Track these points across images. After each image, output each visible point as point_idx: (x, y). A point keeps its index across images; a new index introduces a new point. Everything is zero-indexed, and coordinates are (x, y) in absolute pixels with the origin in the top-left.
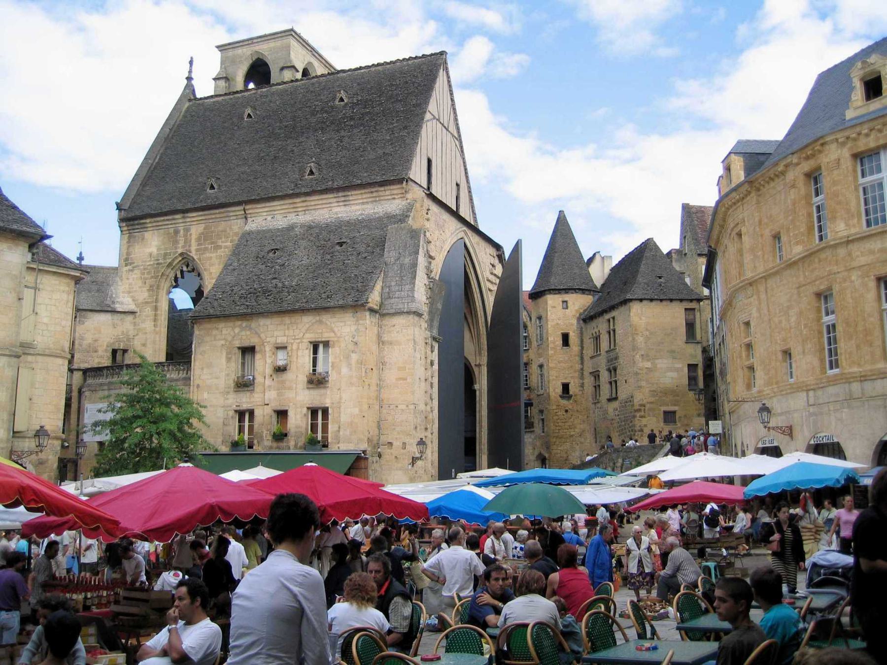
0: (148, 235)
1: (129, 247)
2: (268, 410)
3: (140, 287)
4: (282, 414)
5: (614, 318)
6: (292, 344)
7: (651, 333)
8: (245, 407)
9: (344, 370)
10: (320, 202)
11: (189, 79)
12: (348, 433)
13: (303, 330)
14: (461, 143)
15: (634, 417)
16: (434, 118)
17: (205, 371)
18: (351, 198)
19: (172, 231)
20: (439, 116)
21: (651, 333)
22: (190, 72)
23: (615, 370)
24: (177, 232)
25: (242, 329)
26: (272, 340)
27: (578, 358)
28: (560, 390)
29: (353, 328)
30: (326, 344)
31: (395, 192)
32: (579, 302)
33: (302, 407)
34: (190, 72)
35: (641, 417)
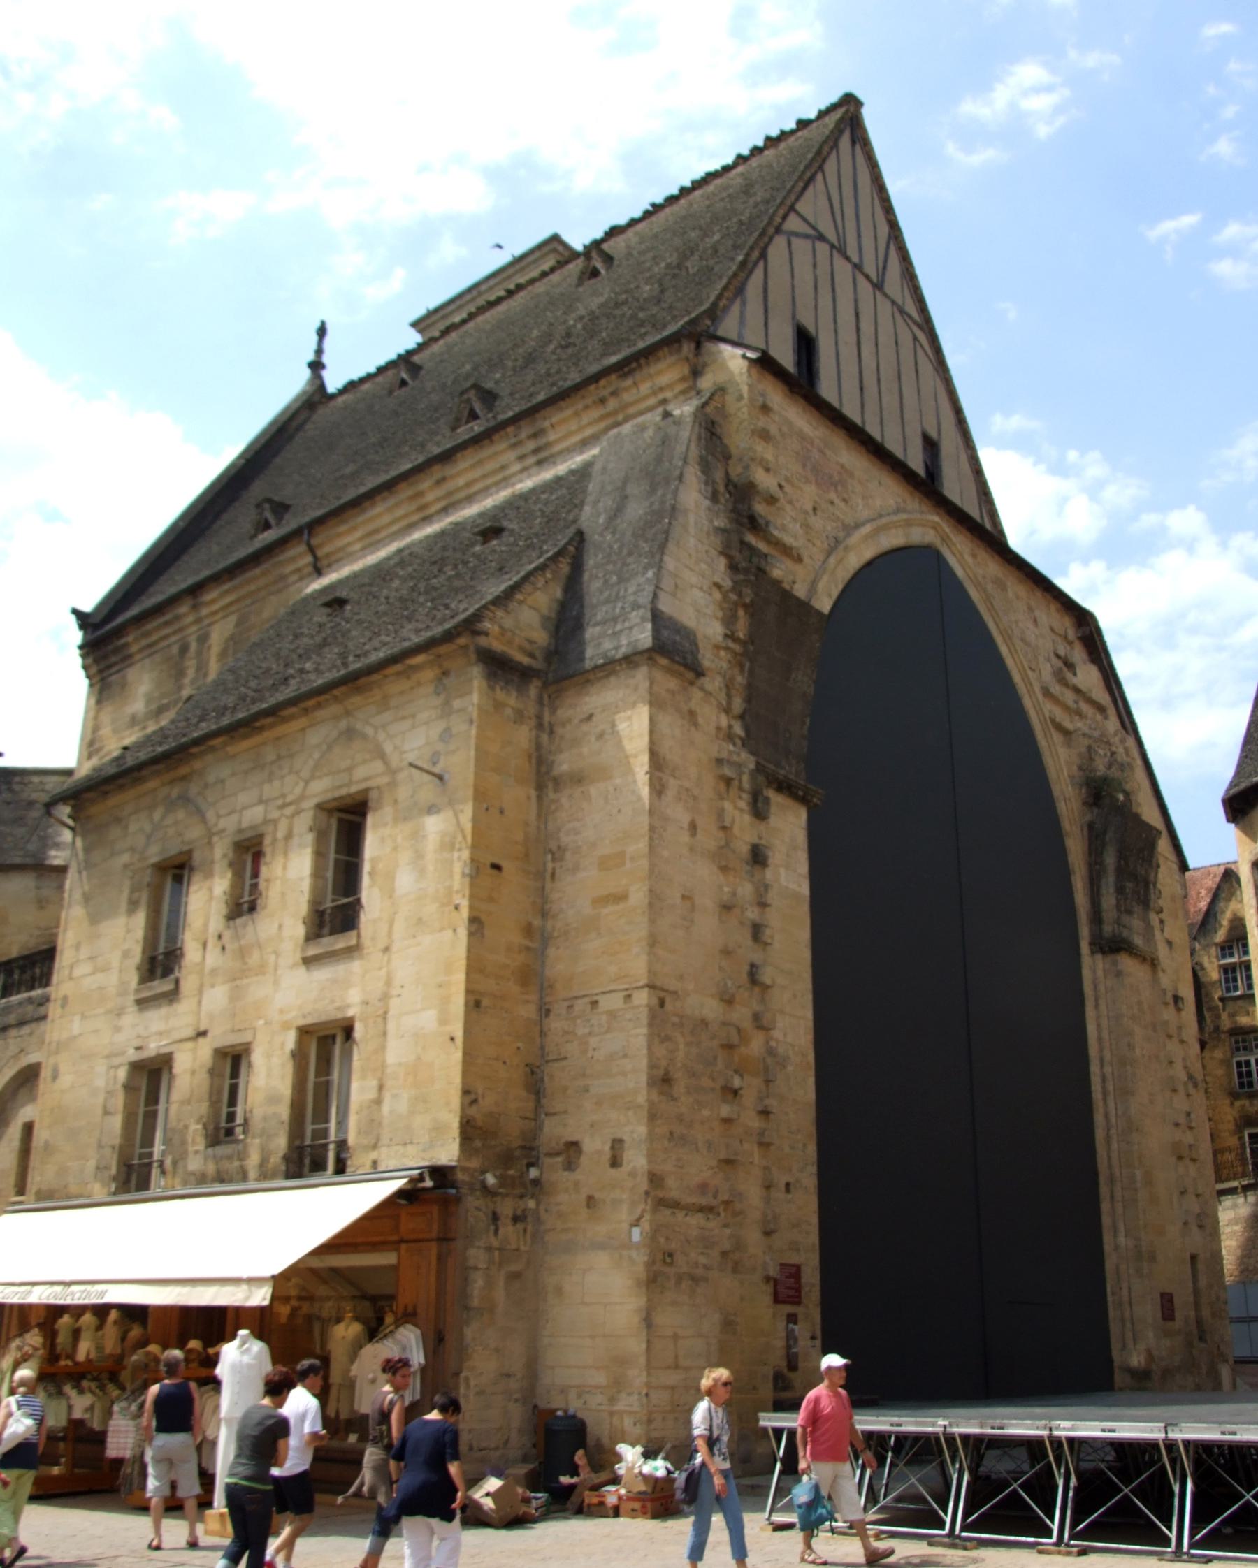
0: (132, 674)
2: (204, 1051)
4: (233, 1061)
6: (275, 822)
8: (154, 1048)
9: (405, 881)
11: (316, 366)
12: (403, 1106)
13: (305, 773)
16: (821, 238)
17: (84, 953)
19: (175, 650)
22: (319, 351)
24: (184, 649)
25: (171, 805)
26: (229, 824)
29: (437, 728)
31: (664, 379)
33: (285, 1026)
34: (319, 351)
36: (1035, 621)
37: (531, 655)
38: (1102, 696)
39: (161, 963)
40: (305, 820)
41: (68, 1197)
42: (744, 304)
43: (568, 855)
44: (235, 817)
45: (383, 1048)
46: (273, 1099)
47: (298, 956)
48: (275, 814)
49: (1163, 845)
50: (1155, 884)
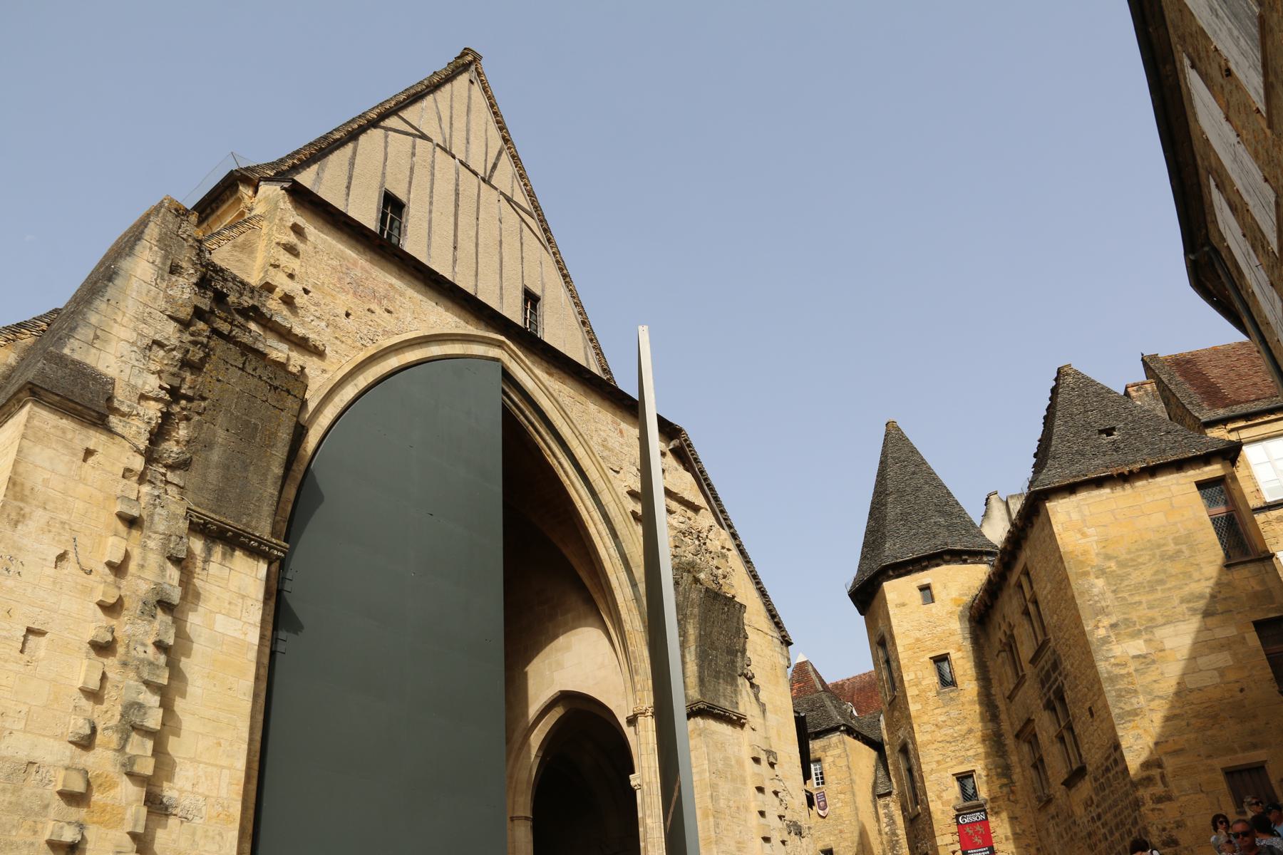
7: (1121, 564)
14: (542, 221)
15: (1137, 804)
16: (424, 137)
21: (1121, 564)
32: (961, 582)
35: (1159, 800)
36: (621, 432)
38: (700, 500)
49: (755, 616)
50: (744, 651)
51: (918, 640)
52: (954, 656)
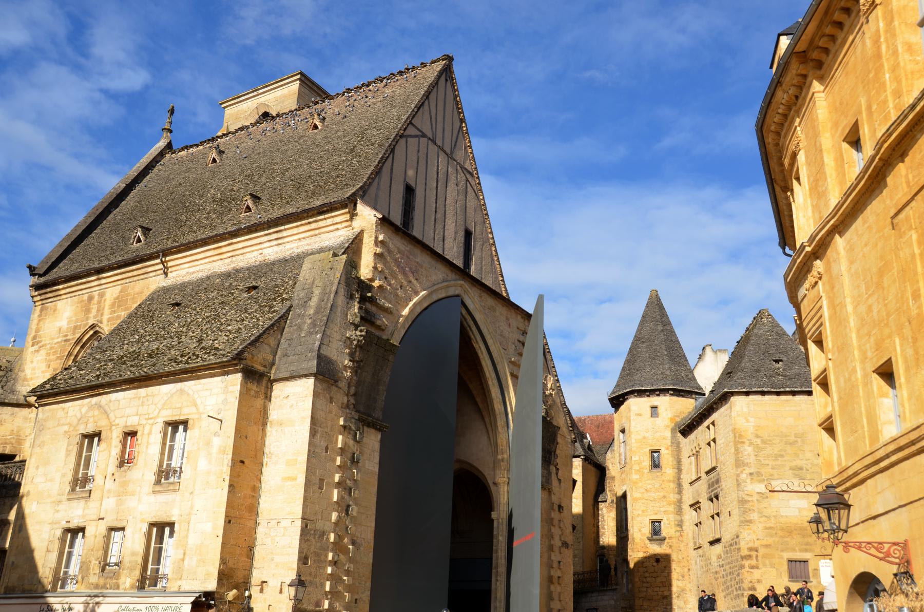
0: (60, 304)
1: (39, 321)
3: (43, 372)
5: (713, 423)
7: (764, 442)
9: (202, 464)
10: (249, 243)
13: (159, 406)
15: (742, 567)
17: (41, 470)
18: (285, 234)
19: (86, 297)
20: (434, 134)
21: (764, 442)
23: (717, 497)
24: (91, 298)
27: (672, 485)
28: (647, 530)
30: (185, 423)
33: (142, 521)
35: (752, 567)
37: (265, 366)
39: (81, 482)
40: (160, 426)
41: (24, 591)
42: (380, 179)
43: (273, 457)
44: (124, 419)
45: (187, 536)
46: (134, 554)
47: (151, 490)
48: (144, 422)
51: (644, 438)
52: (664, 451)
